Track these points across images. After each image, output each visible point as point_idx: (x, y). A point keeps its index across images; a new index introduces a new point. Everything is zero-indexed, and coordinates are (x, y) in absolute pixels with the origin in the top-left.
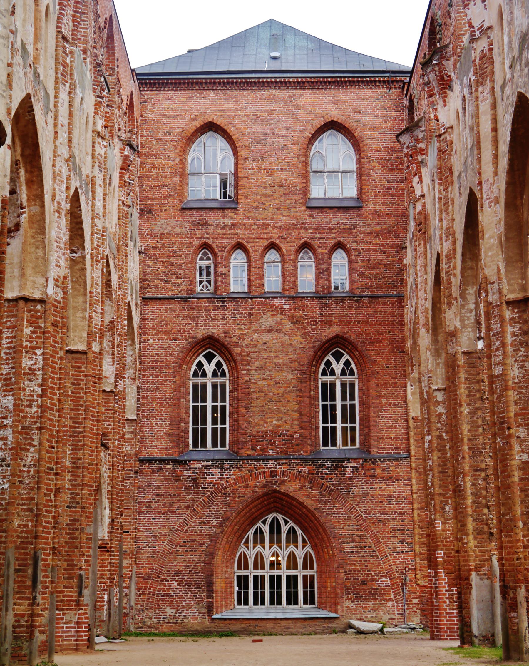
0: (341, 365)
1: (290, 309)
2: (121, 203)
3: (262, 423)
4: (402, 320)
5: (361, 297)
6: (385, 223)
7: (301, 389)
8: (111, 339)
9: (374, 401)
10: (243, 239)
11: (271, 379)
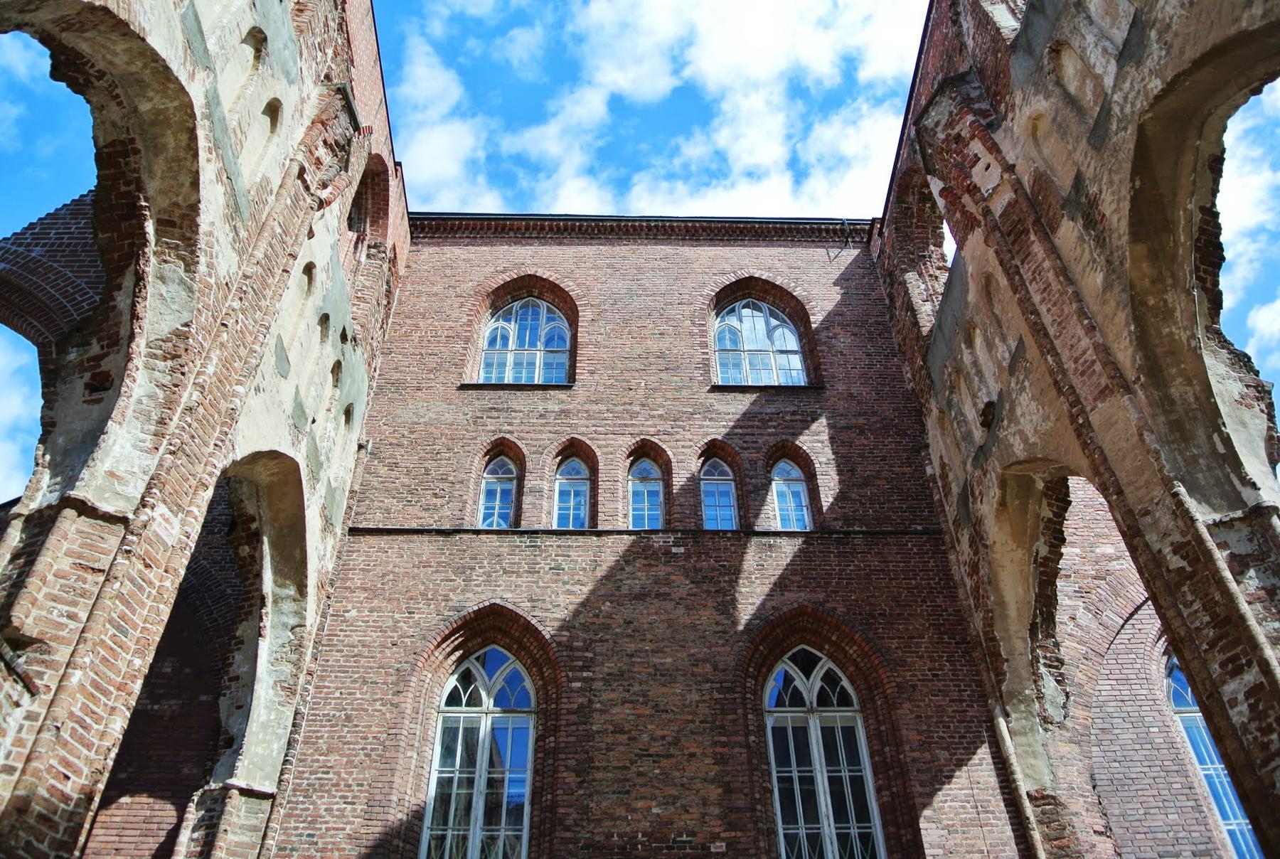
0: (816, 682)
1: (687, 556)
2: (296, 170)
3: (620, 811)
4: (948, 577)
5: (847, 533)
6: (874, 414)
7: (723, 727)
8: (166, 380)
9: (916, 754)
10: (583, 434)
11: (645, 703)
